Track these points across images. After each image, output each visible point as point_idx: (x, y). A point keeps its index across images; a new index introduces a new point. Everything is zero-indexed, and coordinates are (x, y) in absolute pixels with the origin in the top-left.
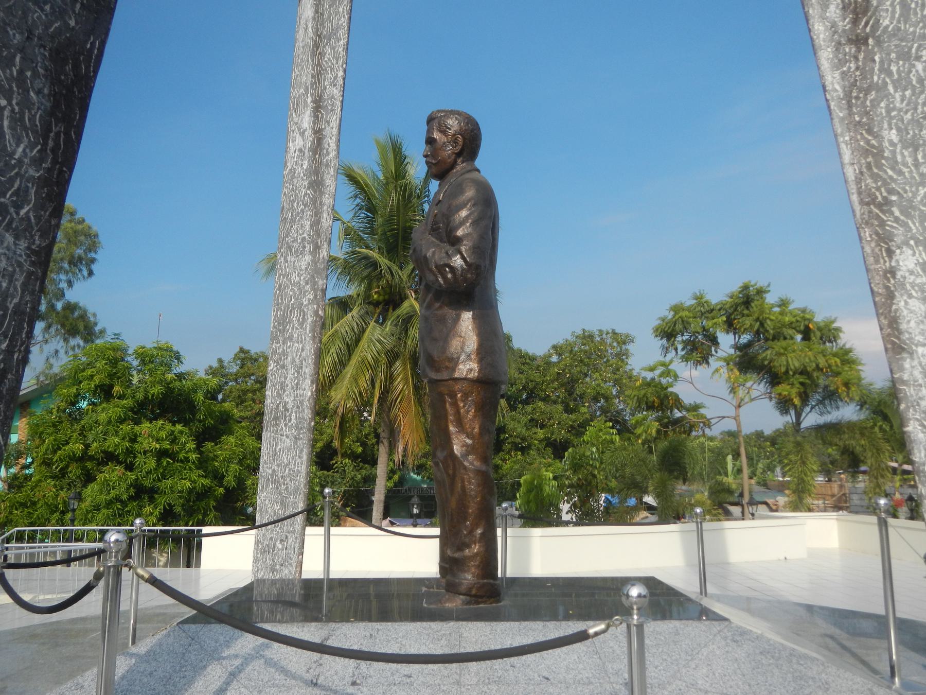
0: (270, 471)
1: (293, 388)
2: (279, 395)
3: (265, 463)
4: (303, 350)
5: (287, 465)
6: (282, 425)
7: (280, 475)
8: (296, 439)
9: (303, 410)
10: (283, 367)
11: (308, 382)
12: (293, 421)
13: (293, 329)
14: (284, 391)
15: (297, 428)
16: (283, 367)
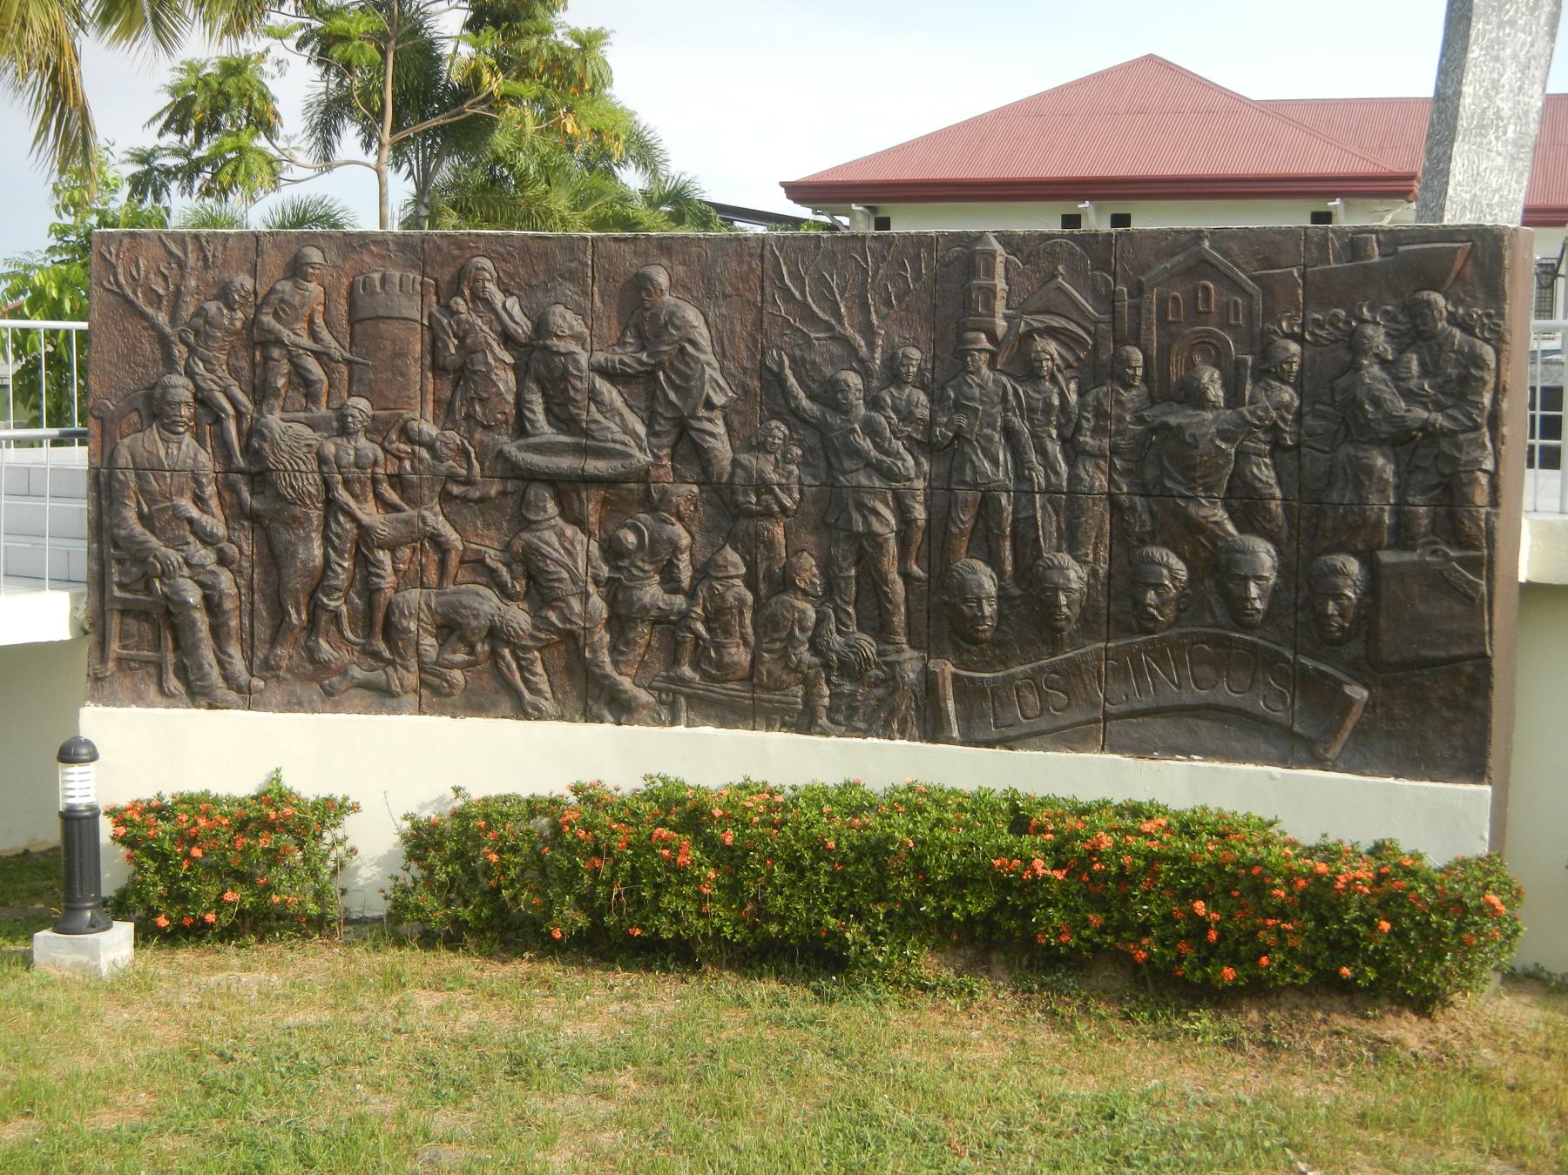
0: (1468, 196)
1: (1512, 91)
2: (1487, 96)
3: (1459, 184)
4: (1532, 45)
5: (1497, 190)
6: (1492, 137)
7: (1484, 203)
8: (1514, 158)
9: (1528, 124)
10: (1497, 59)
11: (1538, 89)
12: (1510, 134)
13: (1517, 11)
14: (1497, 93)
15: (1515, 143)
16: (1497, 59)
